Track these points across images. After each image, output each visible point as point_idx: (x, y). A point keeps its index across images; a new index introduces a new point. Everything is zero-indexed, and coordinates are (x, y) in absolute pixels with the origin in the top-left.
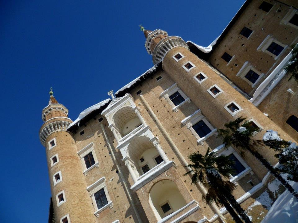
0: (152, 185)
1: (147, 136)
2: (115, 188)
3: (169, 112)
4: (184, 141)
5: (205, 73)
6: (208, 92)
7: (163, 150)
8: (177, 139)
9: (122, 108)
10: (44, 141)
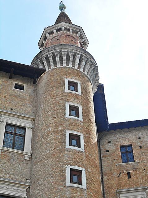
5: (85, 141)
6: (65, 170)
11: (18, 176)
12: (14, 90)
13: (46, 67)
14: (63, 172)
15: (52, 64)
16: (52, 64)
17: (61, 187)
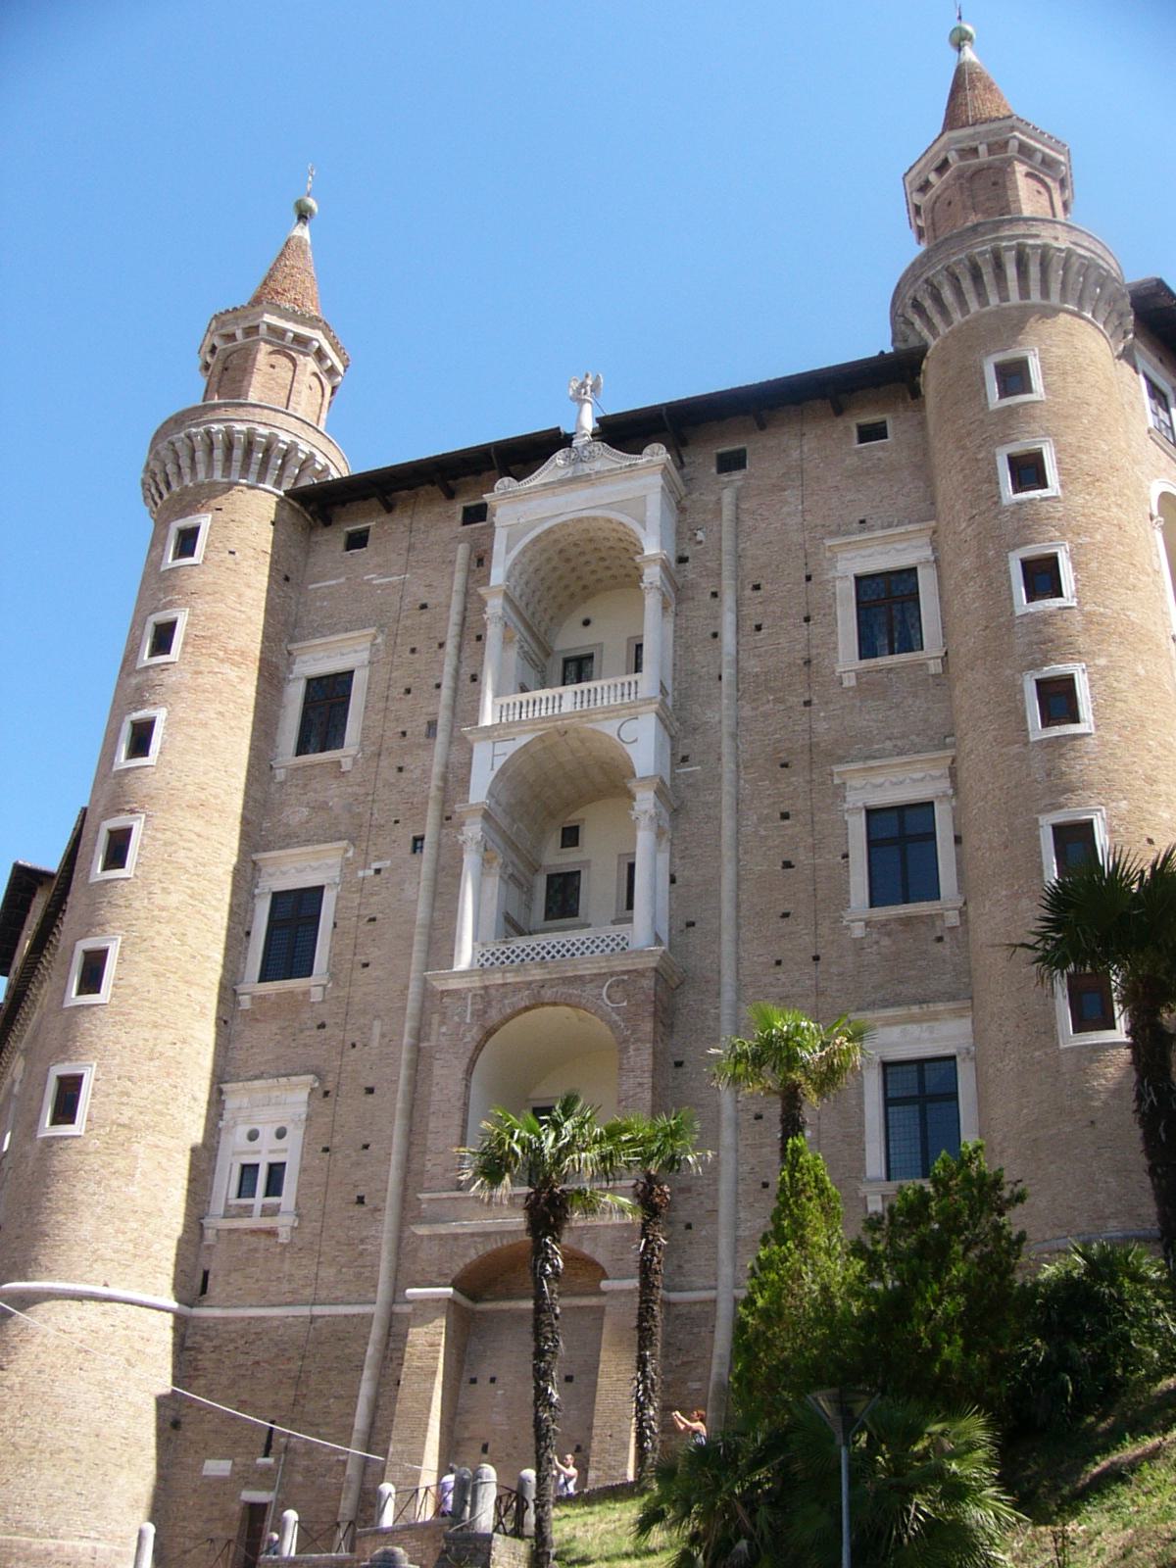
0: (523, 1004)
1: (630, 749)
2: (373, 920)
3: (808, 662)
4: (787, 865)
5: (1076, 567)
6: (1022, 691)
7: (672, 855)
8: (763, 833)
9: (595, 519)
10: (158, 501)
11: (918, 735)
12: (858, 452)
13: (926, 333)
14: (1018, 697)
15: (937, 319)
16: (937, 319)
17: (1016, 749)
